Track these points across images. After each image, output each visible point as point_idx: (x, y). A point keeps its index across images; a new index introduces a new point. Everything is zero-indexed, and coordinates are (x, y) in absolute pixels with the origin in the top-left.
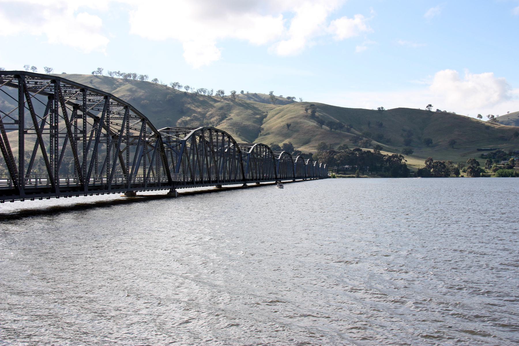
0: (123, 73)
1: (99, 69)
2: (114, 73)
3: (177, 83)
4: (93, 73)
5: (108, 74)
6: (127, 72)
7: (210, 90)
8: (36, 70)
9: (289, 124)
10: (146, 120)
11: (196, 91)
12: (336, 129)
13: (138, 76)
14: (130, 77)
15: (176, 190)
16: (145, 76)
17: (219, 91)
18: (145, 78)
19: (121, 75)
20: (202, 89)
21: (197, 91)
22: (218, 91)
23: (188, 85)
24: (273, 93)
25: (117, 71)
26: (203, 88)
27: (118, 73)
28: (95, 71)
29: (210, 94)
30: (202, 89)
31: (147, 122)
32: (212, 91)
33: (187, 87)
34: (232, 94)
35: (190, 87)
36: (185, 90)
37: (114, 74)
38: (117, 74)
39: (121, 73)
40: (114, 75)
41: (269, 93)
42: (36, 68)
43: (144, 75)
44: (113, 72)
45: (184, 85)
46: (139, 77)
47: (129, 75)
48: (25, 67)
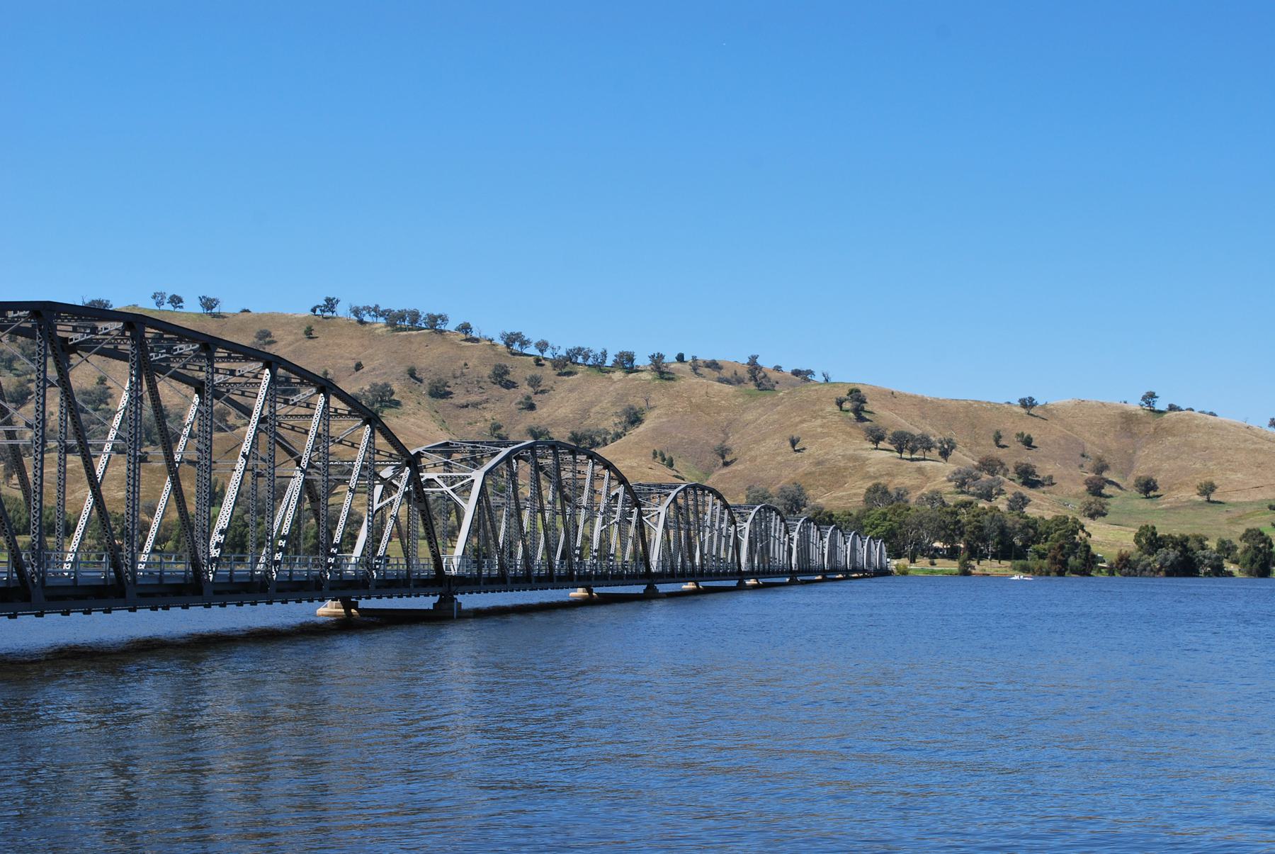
0: (385, 311)
1: (328, 300)
2: (364, 309)
3: (518, 334)
4: (314, 310)
5: (349, 312)
6: (396, 308)
7: (598, 351)
8: (181, 304)
10: (377, 422)
11: (565, 355)
12: (912, 451)
13: (423, 316)
14: (404, 321)
15: (455, 596)
16: (440, 316)
17: (621, 355)
18: (439, 322)
19: (381, 316)
20: (579, 348)
21: (568, 353)
22: (618, 353)
23: (546, 339)
25: (372, 306)
26: (581, 346)
28: (318, 306)
29: (599, 360)
30: (580, 350)
31: (378, 425)
32: (604, 354)
33: (542, 346)
35: (550, 345)
36: (537, 353)
37: (364, 312)
38: (373, 313)
40: (364, 315)
41: (748, 360)
42: (180, 300)
43: (436, 314)
44: (361, 307)
45: (535, 340)
46: (425, 319)
47: (401, 316)
48: (154, 297)
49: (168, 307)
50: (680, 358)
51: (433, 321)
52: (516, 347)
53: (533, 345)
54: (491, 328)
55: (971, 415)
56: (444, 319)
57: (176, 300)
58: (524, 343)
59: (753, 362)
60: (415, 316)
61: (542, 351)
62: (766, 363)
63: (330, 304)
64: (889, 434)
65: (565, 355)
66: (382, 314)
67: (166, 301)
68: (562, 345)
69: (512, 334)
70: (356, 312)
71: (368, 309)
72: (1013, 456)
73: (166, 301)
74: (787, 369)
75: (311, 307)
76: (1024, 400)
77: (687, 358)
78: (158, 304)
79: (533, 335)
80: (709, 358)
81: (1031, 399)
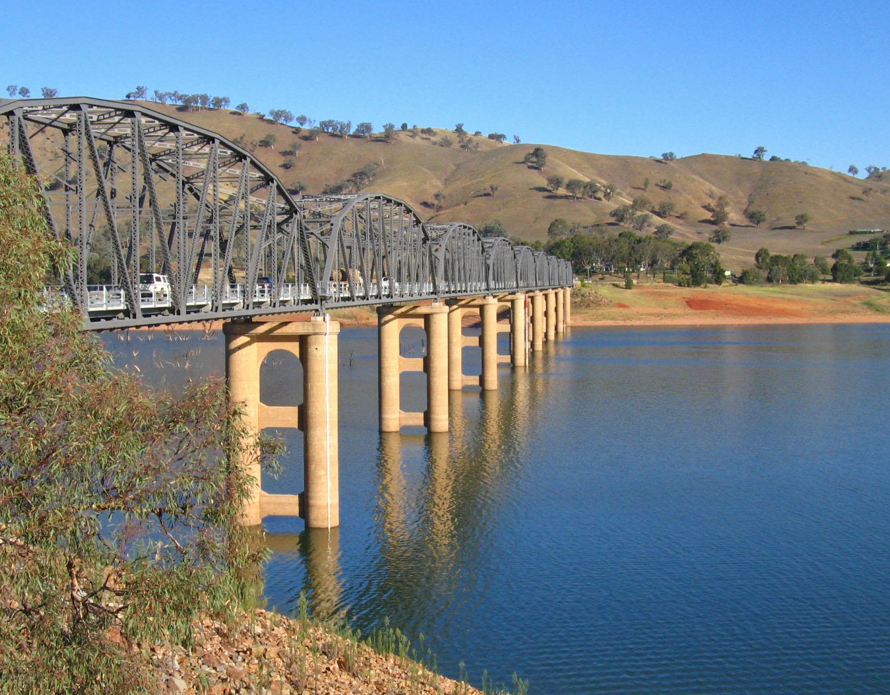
0: (183, 96)
2: (166, 94)
4: (128, 96)
6: (190, 93)
8: (28, 94)
9: (495, 186)
14: (197, 102)
16: (224, 98)
17: (362, 125)
18: (223, 103)
21: (321, 125)
24: (463, 128)
26: (331, 119)
27: (174, 95)
28: (131, 93)
30: (330, 122)
32: (349, 125)
33: (302, 120)
34: (386, 129)
36: (297, 125)
38: (173, 98)
39: (181, 93)
43: (221, 97)
45: (296, 114)
47: (194, 99)
48: (8, 89)
49: (18, 97)
50: (404, 127)
51: (218, 102)
52: (281, 121)
53: (295, 118)
54: (262, 106)
55: (625, 165)
56: (226, 101)
57: (24, 91)
58: (288, 118)
59: (459, 130)
60: (205, 98)
61: (302, 124)
62: (470, 130)
63: (141, 91)
64: (566, 181)
65: (319, 126)
66: (180, 98)
67: (17, 92)
68: (315, 119)
69: (279, 111)
70: (161, 97)
71: (170, 95)
72: (656, 198)
73: (17, 92)
74: (485, 135)
75: (127, 93)
76: (666, 154)
77: (410, 127)
78: (12, 94)
79: (296, 114)
80: (425, 127)
81: (671, 154)
